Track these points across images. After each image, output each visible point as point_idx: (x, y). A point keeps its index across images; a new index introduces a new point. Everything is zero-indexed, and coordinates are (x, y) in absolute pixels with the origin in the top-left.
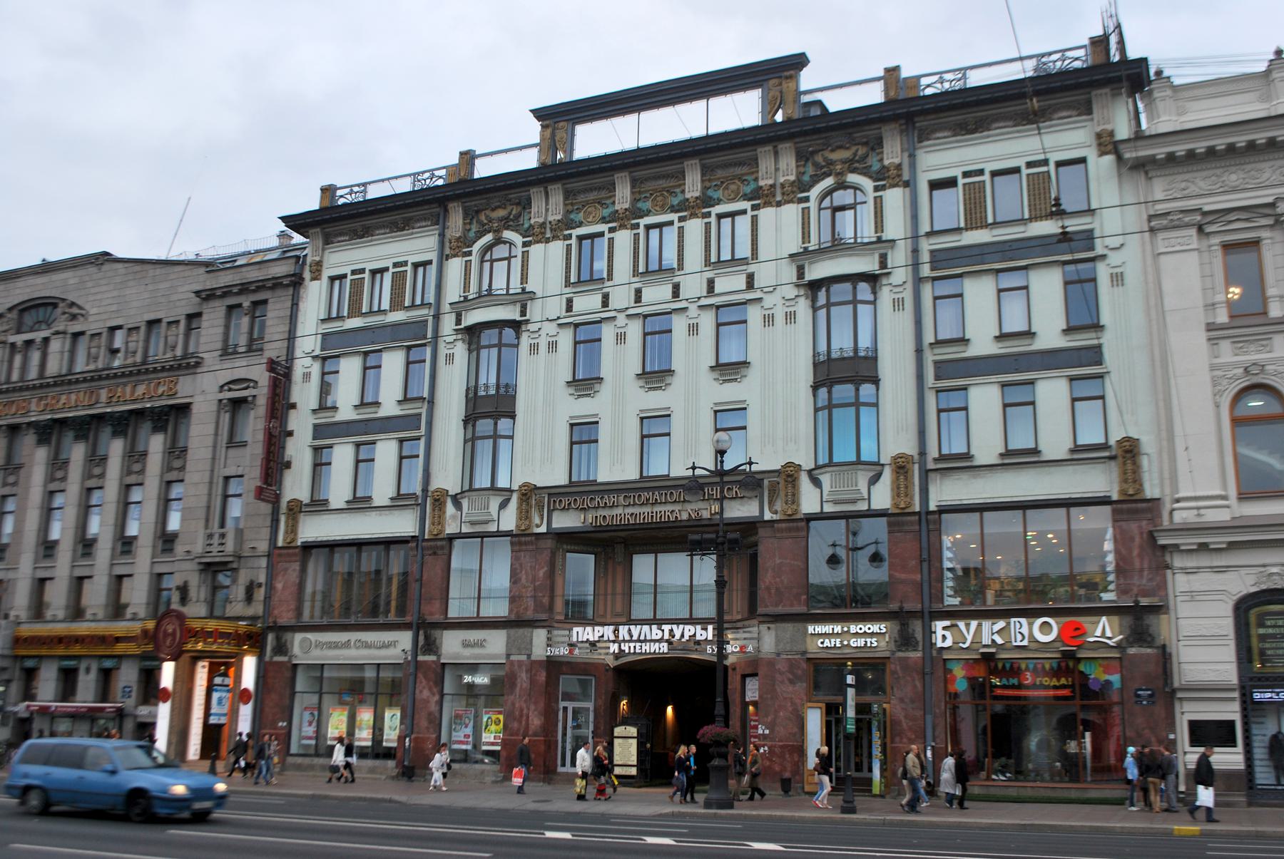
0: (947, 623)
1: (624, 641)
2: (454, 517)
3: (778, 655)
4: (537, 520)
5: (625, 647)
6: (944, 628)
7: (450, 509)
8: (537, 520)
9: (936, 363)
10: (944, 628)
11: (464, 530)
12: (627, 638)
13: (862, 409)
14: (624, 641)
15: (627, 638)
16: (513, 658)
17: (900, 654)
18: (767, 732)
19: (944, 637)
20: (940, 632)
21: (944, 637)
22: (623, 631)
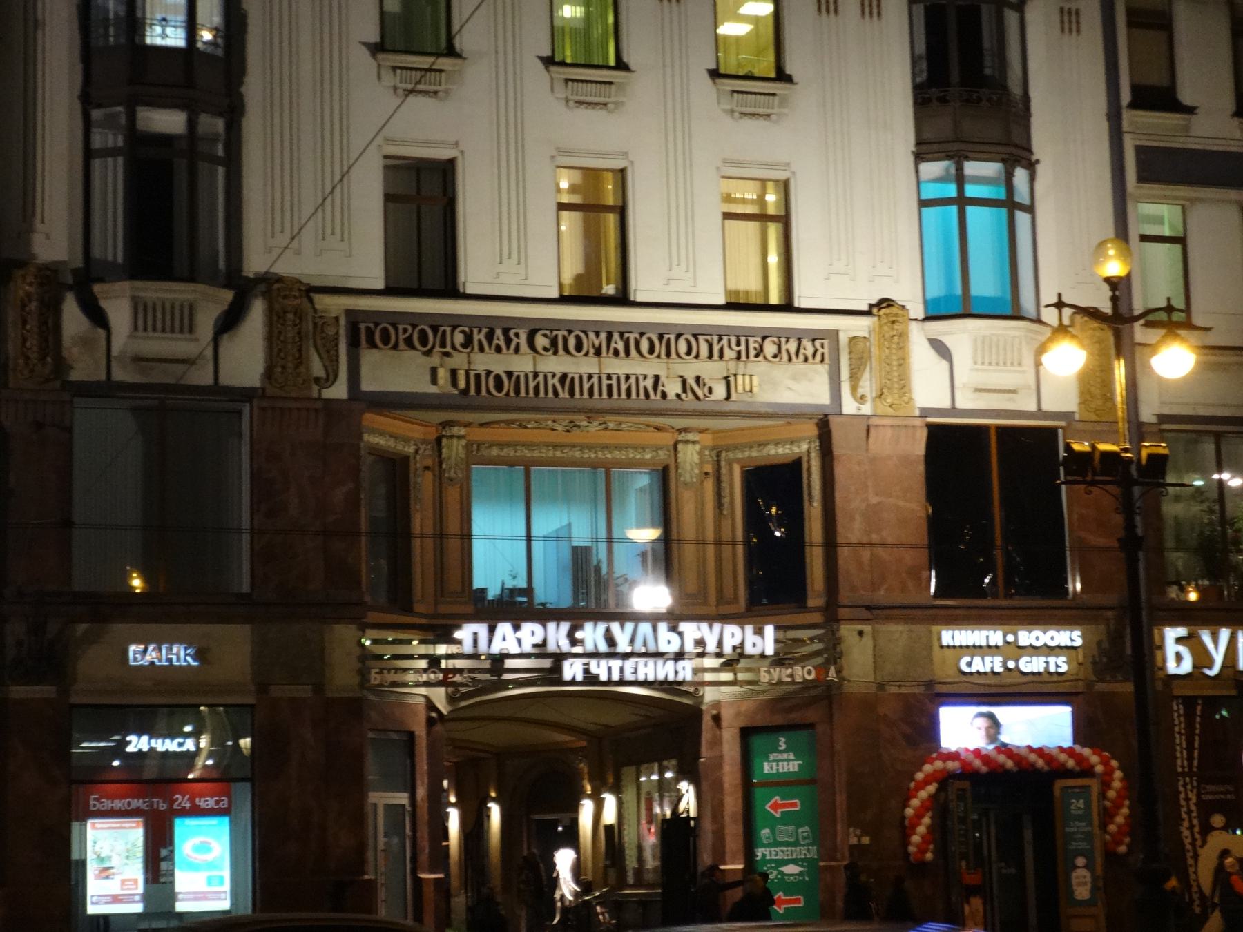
0: (1181, 631)
1: (596, 655)
2: (85, 342)
3: (881, 686)
4: (317, 369)
5: (600, 669)
6: (1179, 640)
7: (73, 318)
8: (317, 369)
9: (1139, 150)
10: (1179, 640)
11: (119, 375)
12: (603, 647)
13: (971, 210)
14: (596, 655)
15: (603, 647)
16: (277, 691)
17: (1100, 687)
18: (866, 840)
19: (1179, 658)
20: (1171, 648)
21: (1179, 658)
22: (592, 635)
